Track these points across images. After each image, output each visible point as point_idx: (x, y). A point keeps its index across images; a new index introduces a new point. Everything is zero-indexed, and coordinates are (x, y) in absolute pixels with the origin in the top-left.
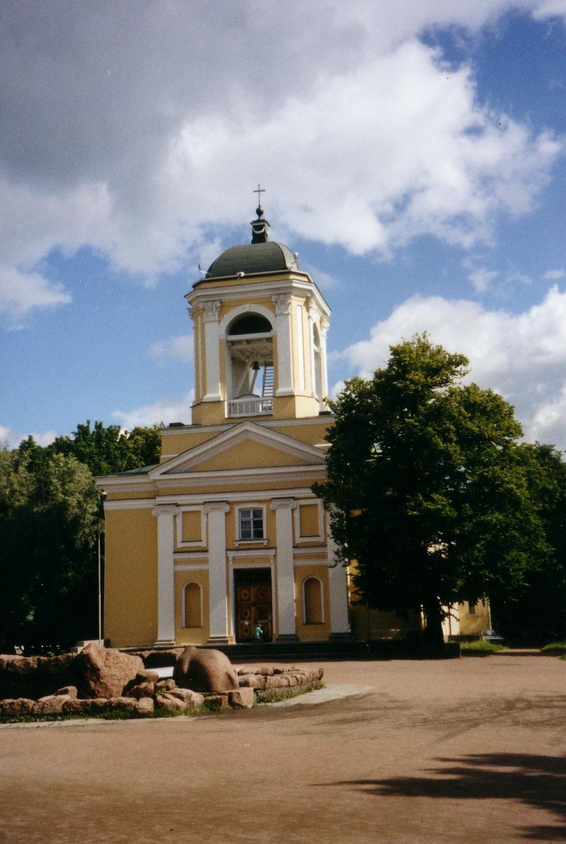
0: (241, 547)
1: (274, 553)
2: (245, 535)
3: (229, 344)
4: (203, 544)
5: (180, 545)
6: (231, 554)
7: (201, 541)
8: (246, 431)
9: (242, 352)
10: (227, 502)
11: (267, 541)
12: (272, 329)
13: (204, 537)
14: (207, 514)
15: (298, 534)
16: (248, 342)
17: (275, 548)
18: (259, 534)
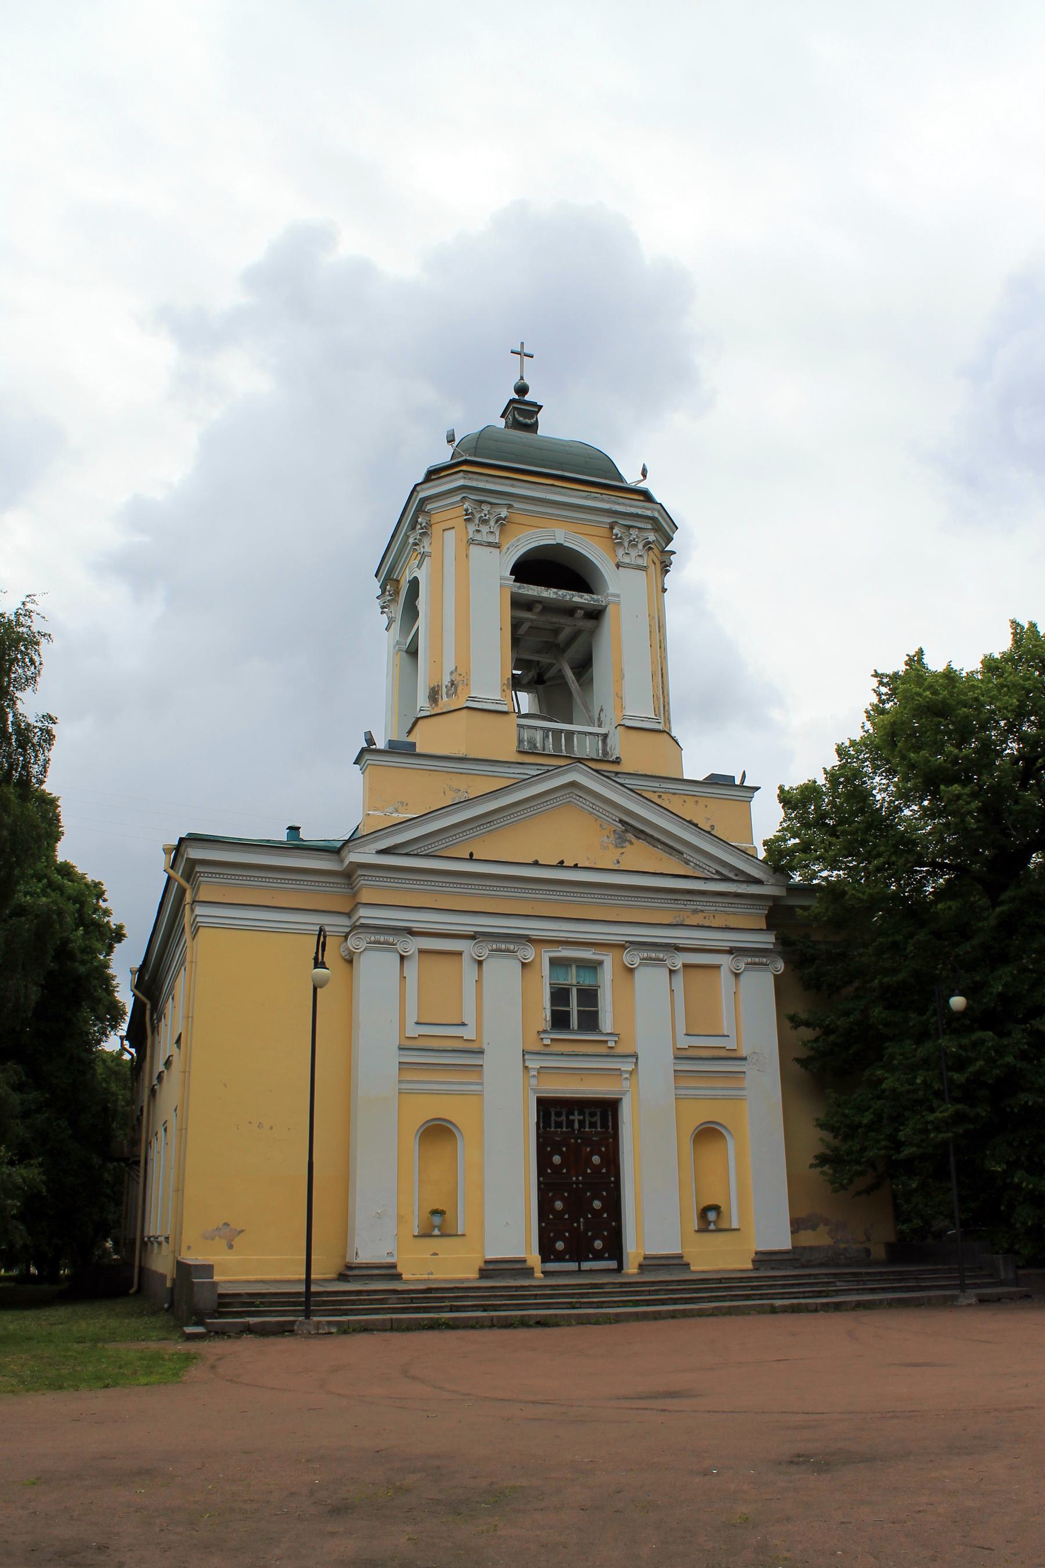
1: (630, 1067)
2: (560, 1021)
4: (469, 1033)
5: (413, 1031)
6: (534, 1064)
7: (463, 1024)
8: (573, 784)
10: (529, 940)
13: (469, 1015)
14: (480, 963)
15: (681, 1029)
17: (635, 1056)
18: (590, 1021)
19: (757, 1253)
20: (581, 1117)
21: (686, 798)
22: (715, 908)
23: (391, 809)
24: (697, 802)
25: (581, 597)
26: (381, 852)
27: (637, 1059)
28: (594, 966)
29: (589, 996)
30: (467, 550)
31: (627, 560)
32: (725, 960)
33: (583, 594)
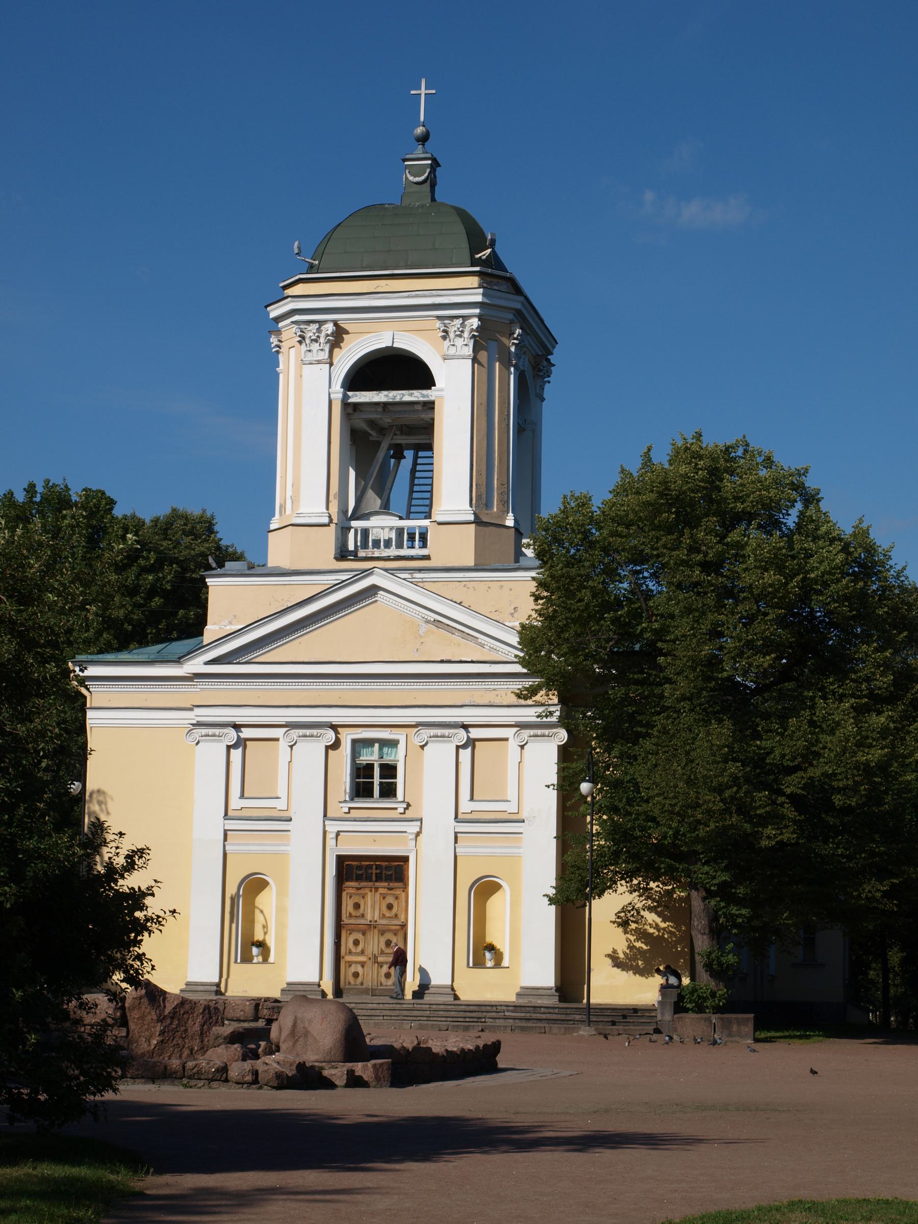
0: (354, 814)
2: (361, 790)
3: (350, 410)
4: (281, 804)
6: (332, 827)
9: (372, 423)
11: (405, 806)
12: (435, 385)
13: (281, 791)
16: (385, 405)
17: (421, 820)
18: (389, 791)
19: (522, 988)
20: (378, 871)
21: (490, 584)
22: (507, 687)
23: (226, 622)
24: (502, 587)
25: (411, 395)
26: (208, 663)
27: (421, 823)
28: (394, 744)
29: (389, 770)
30: (301, 368)
31: (452, 351)
32: (509, 733)
33: (413, 392)
